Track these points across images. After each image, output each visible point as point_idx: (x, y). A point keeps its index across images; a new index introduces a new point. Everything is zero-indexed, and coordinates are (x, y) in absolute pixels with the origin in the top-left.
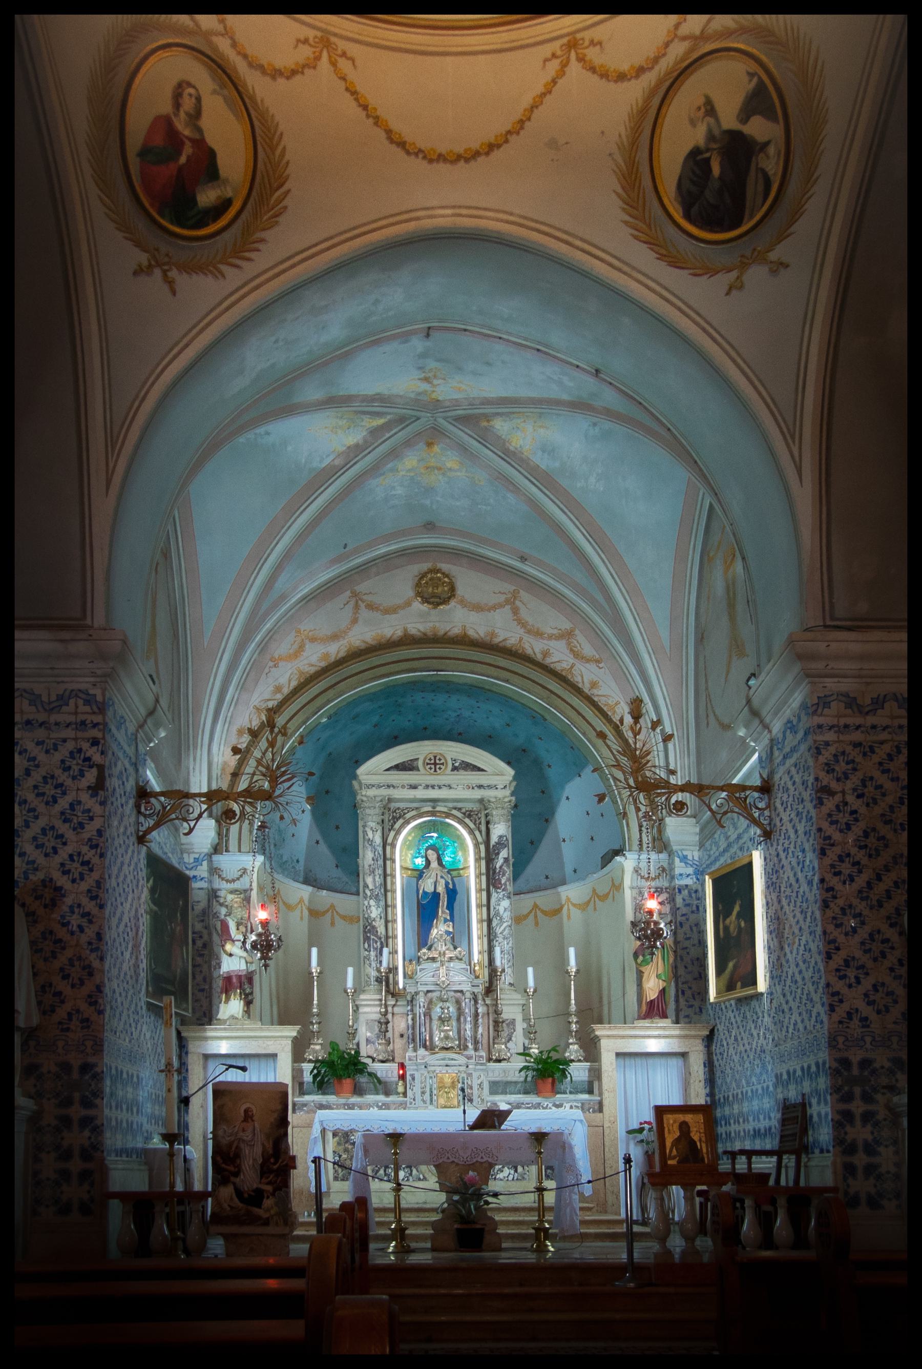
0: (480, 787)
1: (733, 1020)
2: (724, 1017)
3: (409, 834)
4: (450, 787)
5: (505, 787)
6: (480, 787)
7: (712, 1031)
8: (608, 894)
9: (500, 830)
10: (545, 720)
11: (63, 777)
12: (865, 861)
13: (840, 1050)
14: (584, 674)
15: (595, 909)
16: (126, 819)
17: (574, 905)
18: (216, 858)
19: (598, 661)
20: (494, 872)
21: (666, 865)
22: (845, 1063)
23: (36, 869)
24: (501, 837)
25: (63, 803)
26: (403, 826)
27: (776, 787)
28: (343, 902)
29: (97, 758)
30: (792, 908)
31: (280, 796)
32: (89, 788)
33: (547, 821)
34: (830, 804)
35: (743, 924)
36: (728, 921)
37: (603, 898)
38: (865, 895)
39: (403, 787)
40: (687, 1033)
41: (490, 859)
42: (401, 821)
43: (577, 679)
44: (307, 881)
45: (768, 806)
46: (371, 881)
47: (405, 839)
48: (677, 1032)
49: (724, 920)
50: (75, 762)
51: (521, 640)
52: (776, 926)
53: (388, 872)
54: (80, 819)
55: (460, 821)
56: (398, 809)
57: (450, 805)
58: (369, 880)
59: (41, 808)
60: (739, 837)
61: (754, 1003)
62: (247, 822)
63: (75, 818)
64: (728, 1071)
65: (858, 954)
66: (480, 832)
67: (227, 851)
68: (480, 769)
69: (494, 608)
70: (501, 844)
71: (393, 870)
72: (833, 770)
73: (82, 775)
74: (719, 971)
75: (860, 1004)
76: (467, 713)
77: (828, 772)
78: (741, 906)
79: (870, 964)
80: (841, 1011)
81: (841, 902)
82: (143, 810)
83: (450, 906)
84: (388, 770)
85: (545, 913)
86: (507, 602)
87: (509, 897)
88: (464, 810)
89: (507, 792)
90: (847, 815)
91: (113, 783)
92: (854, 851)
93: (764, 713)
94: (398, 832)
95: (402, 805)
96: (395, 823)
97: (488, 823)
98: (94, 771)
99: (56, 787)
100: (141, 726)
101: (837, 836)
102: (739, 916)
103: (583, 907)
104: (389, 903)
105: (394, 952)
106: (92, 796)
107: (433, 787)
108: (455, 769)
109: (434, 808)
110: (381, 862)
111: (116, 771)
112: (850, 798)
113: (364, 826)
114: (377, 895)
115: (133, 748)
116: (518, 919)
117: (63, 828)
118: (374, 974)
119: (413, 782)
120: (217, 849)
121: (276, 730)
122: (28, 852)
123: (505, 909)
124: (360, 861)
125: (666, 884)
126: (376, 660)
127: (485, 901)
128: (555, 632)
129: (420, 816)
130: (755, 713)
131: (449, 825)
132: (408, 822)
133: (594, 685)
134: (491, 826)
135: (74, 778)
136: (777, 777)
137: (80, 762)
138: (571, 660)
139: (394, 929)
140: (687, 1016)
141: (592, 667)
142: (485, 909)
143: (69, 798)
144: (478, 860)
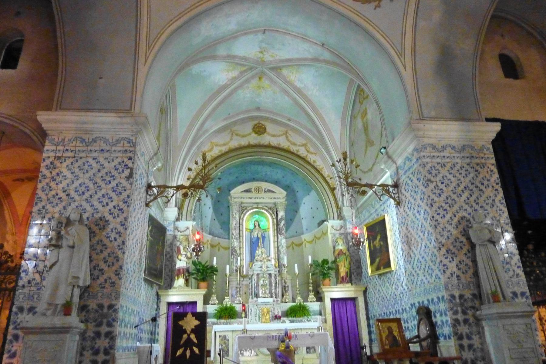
0: (274, 198)
1: (377, 282)
2: (372, 282)
3: (248, 216)
4: (263, 198)
5: (283, 198)
6: (274, 198)
7: (366, 288)
8: (321, 237)
9: (281, 214)
10: (297, 174)
11: (114, 173)
12: (448, 209)
13: (450, 291)
14: (311, 158)
15: (315, 242)
16: (141, 194)
17: (307, 242)
18: (177, 223)
19: (315, 154)
20: (280, 228)
21: (343, 225)
22: (453, 296)
23: (98, 212)
24: (282, 216)
25: (113, 184)
26: (246, 212)
27: (401, 184)
28: (224, 242)
29: (130, 165)
30: (415, 231)
31: (207, 187)
32: (126, 177)
33: (296, 212)
34: (432, 186)
35: (382, 243)
36: (375, 242)
37: (319, 238)
38: (450, 223)
39: (247, 198)
40: (357, 289)
41: (278, 225)
42: (245, 211)
43: (309, 160)
44: (210, 234)
45: (398, 193)
46: (235, 233)
47: (247, 218)
48: (353, 289)
49: (373, 242)
50: (120, 166)
51: (289, 146)
52: (406, 240)
53: (241, 229)
54: (120, 191)
55: (267, 211)
57: (263, 205)
58: (234, 232)
59: (103, 185)
60: (376, 211)
61: (389, 275)
62: (193, 198)
63: (118, 190)
64: (375, 304)
65: (451, 247)
67: (181, 220)
68: (274, 192)
69: (280, 136)
70: (282, 219)
71: (242, 228)
72: (431, 173)
73: (123, 171)
74: (372, 262)
75: (455, 270)
76: (269, 173)
77: (429, 173)
78: (381, 237)
79: (456, 252)
80: (448, 273)
81: (441, 226)
82: (149, 193)
83: (263, 242)
84: (241, 192)
85: (296, 245)
86: (284, 134)
87: (285, 238)
89: (284, 200)
90: (439, 191)
91: (136, 176)
92: (443, 205)
93: (394, 157)
94: (245, 215)
95: (246, 205)
97: (277, 211)
98: (129, 170)
99: (111, 177)
100: (151, 159)
101: (436, 199)
102: (380, 240)
103: (311, 242)
104: (241, 241)
105: (242, 260)
106: (126, 181)
107: (257, 198)
108: (265, 192)
110: (238, 225)
111: (139, 173)
112: (439, 184)
113: (232, 212)
115: (147, 166)
116: (288, 247)
117: (113, 195)
118: (235, 268)
119: (250, 196)
120: (177, 219)
121: (206, 162)
122: (95, 205)
124: (230, 226)
125: (343, 232)
126: (238, 153)
127: (276, 240)
128: (301, 144)
129: (253, 209)
130: (390, 157)
131: (262, 213)
132: (248, 211)
133: (314, 162)
134: (278, 212)
135: (119, 173)
136: (401, 181)
137: (123, 167)
138: (306, 153)
139: (243, 251)
140: (355, 283)
141: (314, 155)
142: (276, 243)
143: (116, 182)
144: (273, 225)
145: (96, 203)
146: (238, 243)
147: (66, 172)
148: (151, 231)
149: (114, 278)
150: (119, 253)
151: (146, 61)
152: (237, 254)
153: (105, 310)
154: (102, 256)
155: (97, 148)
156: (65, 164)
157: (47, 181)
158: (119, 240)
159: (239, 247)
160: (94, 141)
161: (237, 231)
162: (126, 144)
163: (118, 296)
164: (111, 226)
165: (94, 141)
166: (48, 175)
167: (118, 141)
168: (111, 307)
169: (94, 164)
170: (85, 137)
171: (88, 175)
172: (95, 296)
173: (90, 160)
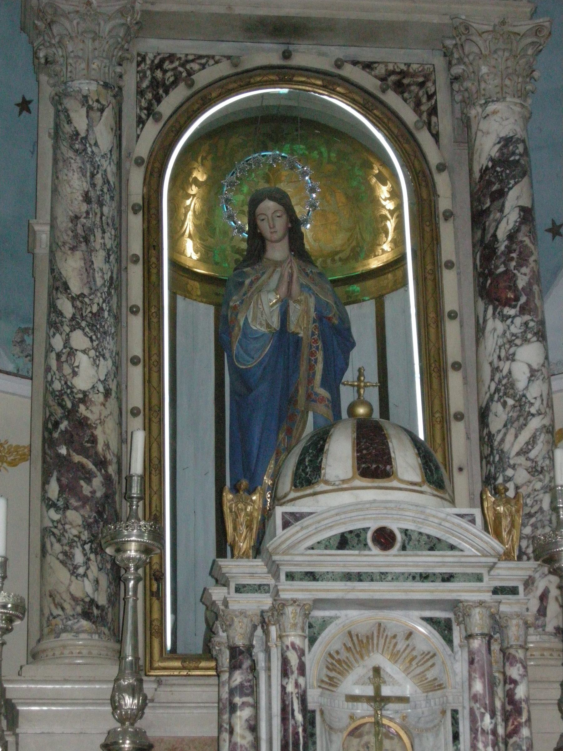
24: (507, 141)
56: (171, 57)
57: (338, 52)
66: (436, 137)
88: (381, 70)
96: (159, 100)
109: (287, 55)
114: (97, 315)
123: (533, 373)
146: (106, 366)
152: (102, 464)
159: (112, 402)
161: (99, 260)
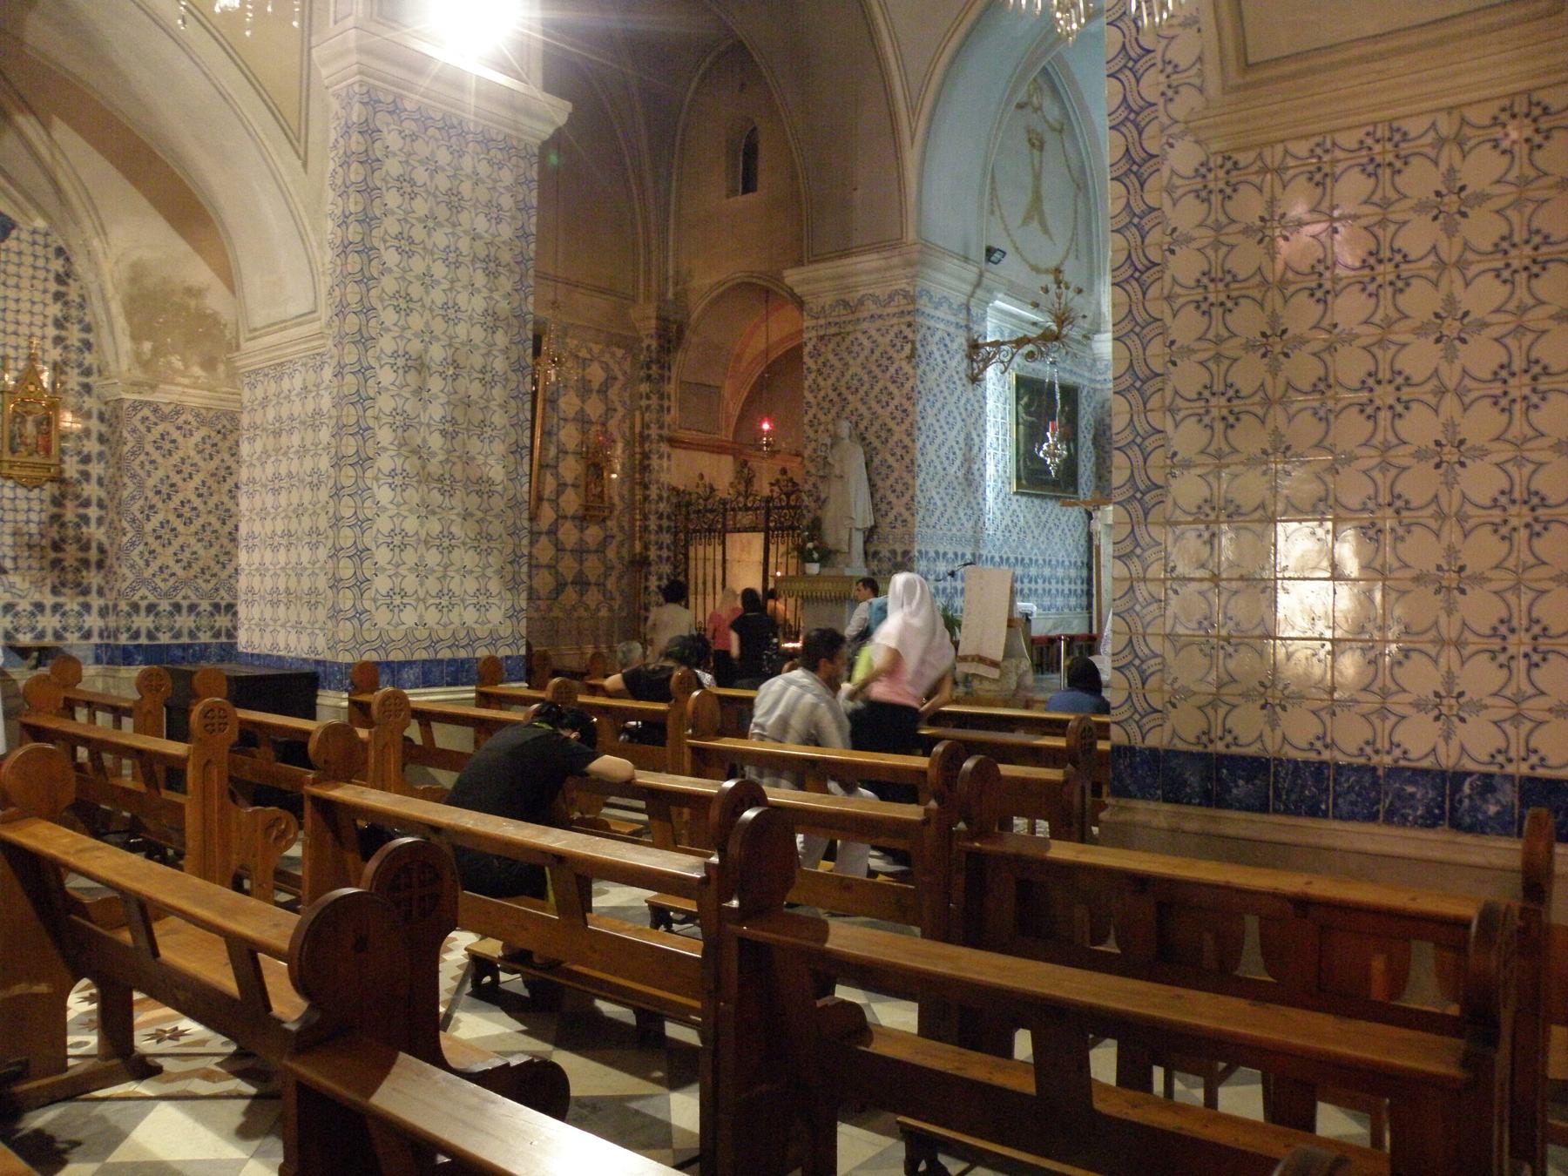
11: (892, 352)
25: (892, 370)
29: (911, 336)
143: (895, 366)
145: (873, 404)
147: (833, 360)
148: (1027, 407)
149: (906, 515)
150: (907, 478)
151: (913, 138)
153: (899, 559)
154: (889, 482)
155: (866, 314)
156: (831, 346)
157: (813, 375)
158: (907, 459)
160: (861, 302)
162: (903, 302)
163: (912, 541)
164: (895, 438)
165: (861, 302)
166: (814, 367)
167: (891, 297)
168: (906, 553)
169: (866, 342)
170: (847, 297)
171: (859, 360)
172: (886, 540)
173: (859, 335)
